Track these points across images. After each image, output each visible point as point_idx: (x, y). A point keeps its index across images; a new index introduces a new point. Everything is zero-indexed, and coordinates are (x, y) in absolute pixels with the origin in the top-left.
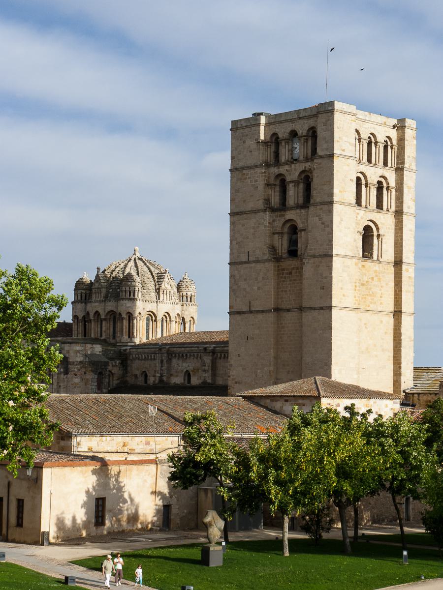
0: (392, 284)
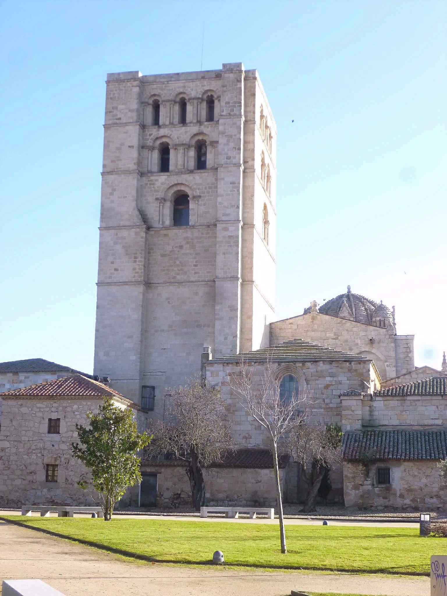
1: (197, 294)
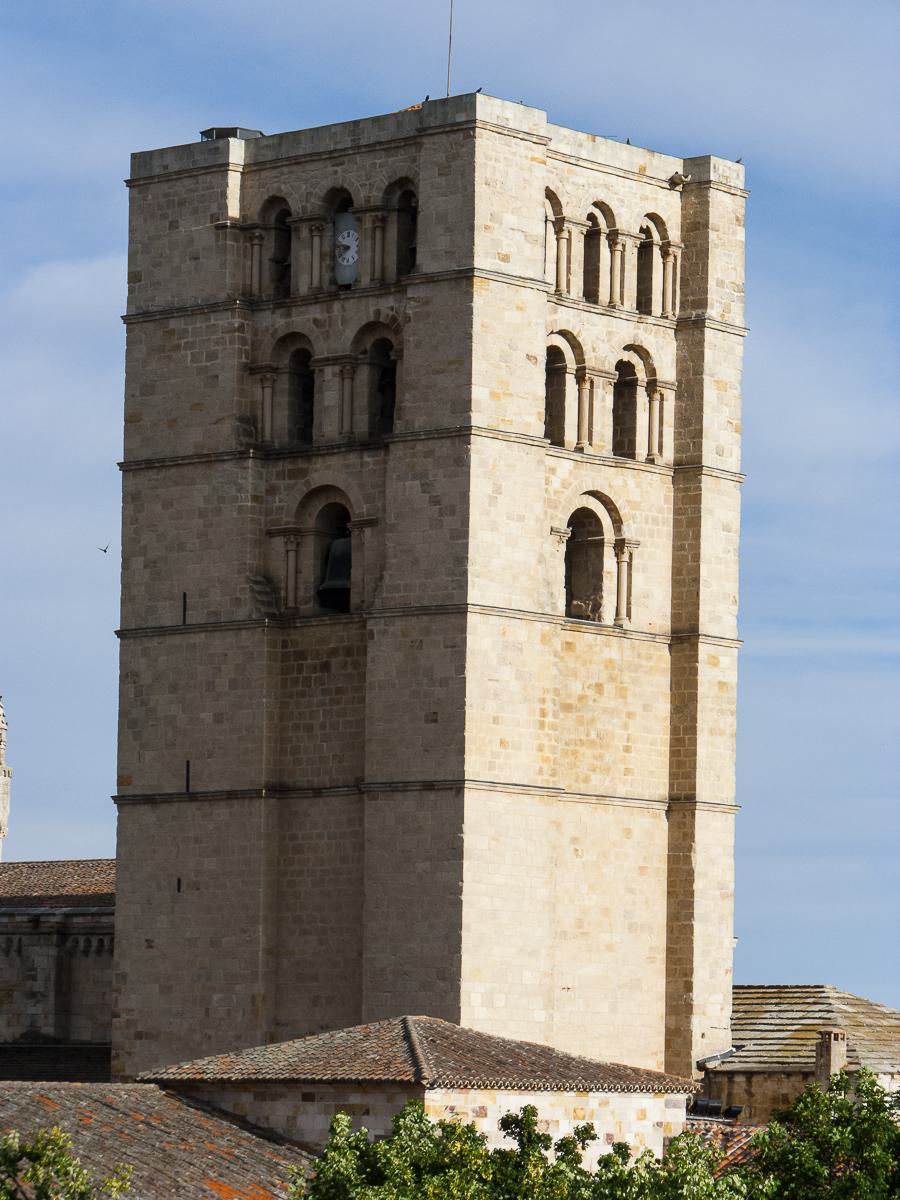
0: (663, 707)
1: (628, 832)
